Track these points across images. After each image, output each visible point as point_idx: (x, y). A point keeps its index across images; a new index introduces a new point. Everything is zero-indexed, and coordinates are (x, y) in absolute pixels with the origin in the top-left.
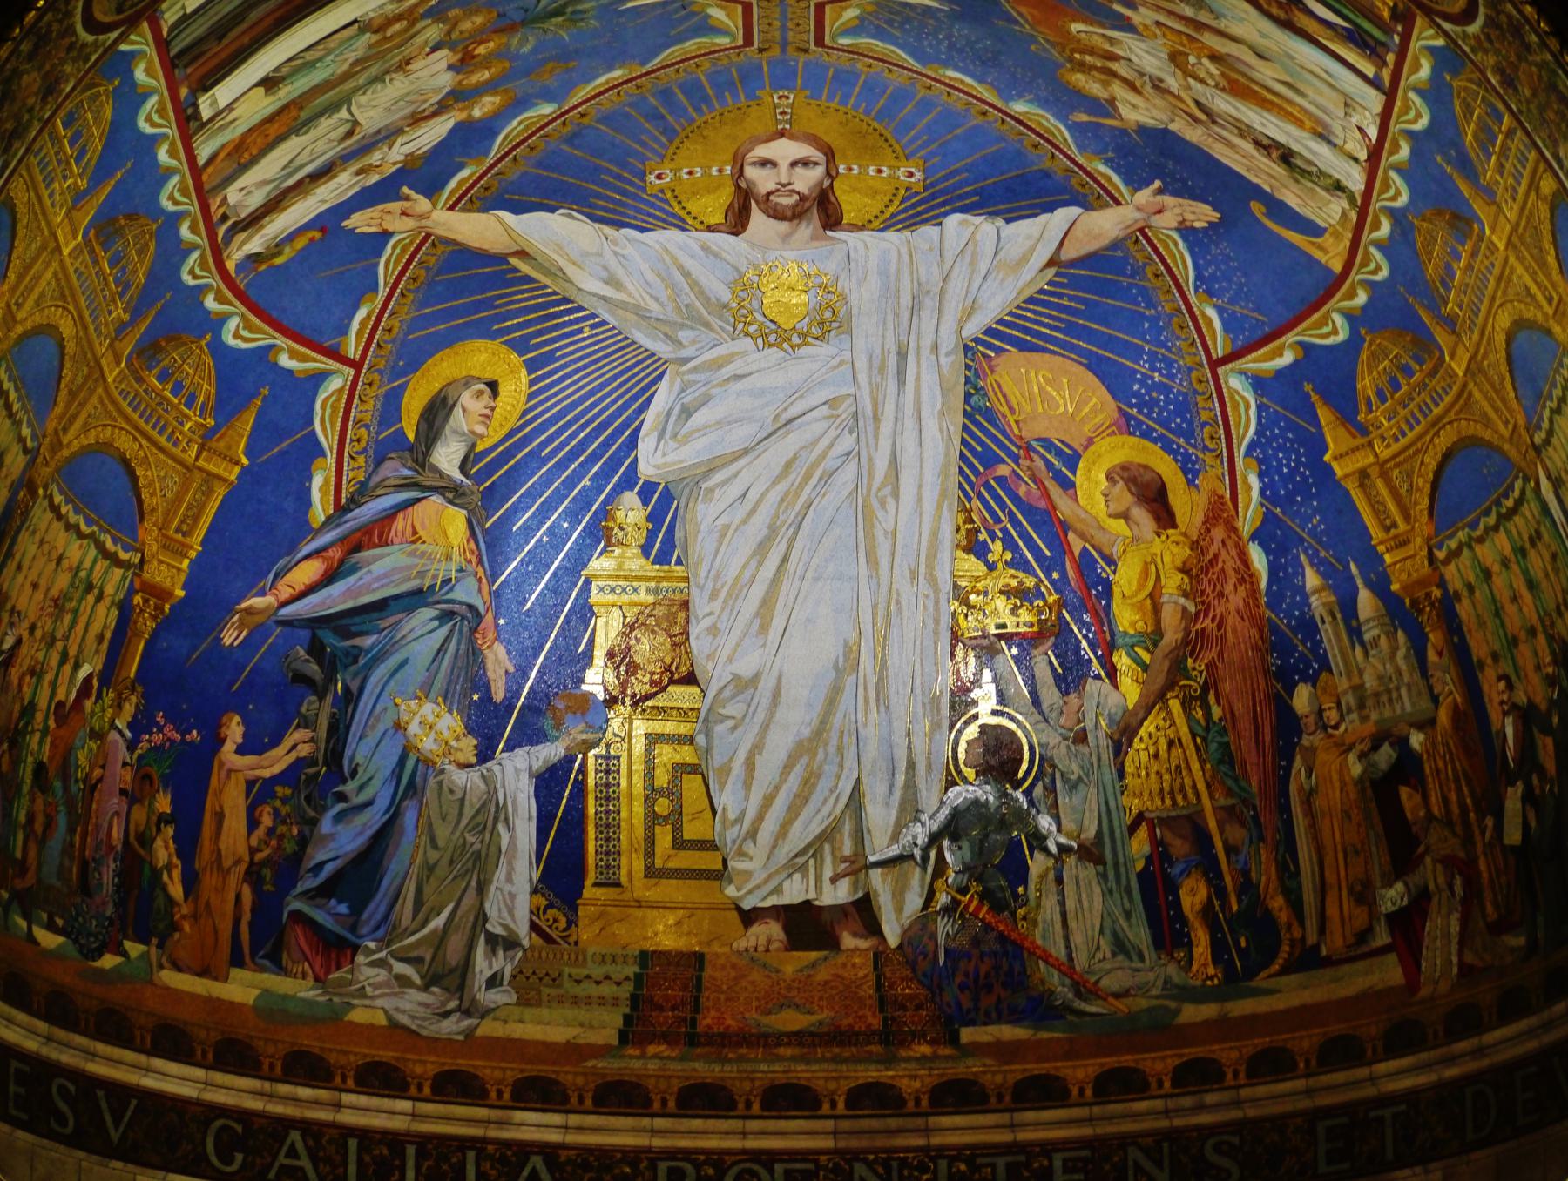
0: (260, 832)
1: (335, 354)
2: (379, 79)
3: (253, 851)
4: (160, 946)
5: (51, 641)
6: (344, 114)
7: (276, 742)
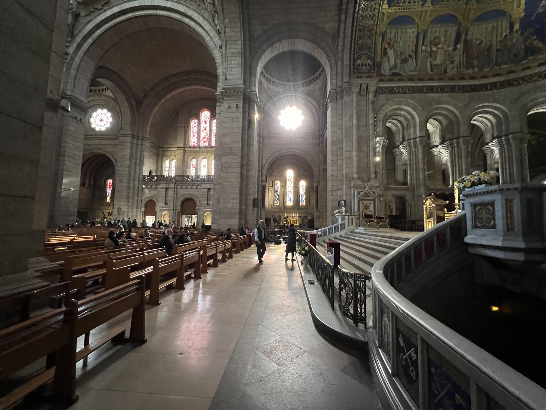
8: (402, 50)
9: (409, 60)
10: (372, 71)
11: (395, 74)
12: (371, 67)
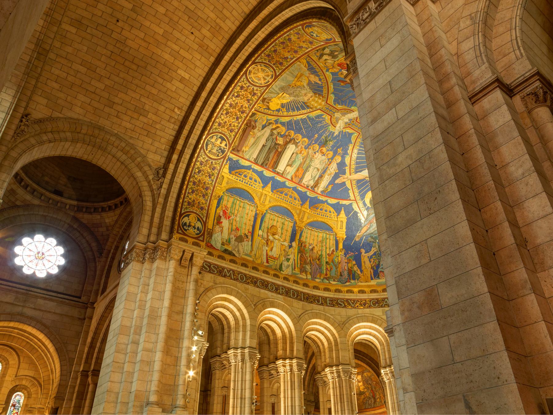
0: (372, 262)
1: (350, 200)
2: (311, 160)
3: (371, 265)
4: (358, 280)
5: (322, 246)
6: (312, 167)
7: (371, 250)
8: (238, 226)
9: (245, 240)
10: (201, 239)
11: (226, 251)
12: (200, 233)
